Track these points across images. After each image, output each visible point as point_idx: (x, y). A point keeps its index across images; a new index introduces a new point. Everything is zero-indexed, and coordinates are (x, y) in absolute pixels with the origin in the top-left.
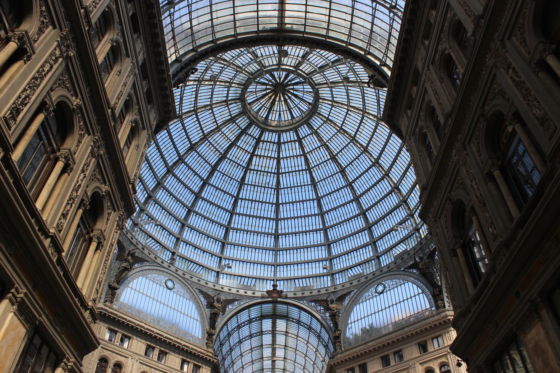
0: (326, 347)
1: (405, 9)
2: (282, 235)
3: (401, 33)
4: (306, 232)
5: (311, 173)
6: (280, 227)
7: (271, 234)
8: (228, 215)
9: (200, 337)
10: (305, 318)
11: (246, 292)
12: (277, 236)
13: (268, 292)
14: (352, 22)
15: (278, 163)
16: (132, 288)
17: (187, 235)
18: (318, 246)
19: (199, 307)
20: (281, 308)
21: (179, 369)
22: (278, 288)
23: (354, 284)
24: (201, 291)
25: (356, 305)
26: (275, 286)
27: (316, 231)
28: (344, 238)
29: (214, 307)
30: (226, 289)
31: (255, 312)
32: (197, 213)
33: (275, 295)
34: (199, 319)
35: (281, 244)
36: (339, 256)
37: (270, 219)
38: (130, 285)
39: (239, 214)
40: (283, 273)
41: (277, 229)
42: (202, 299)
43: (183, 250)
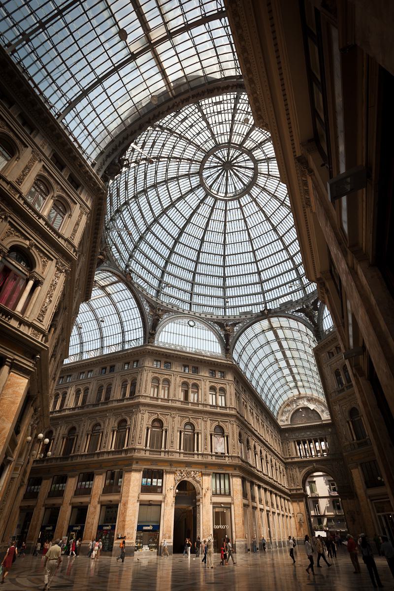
2: (262, 271)
4: (279, 264)
5: (270, 222)
7: (255, 273)
9: (220, 352)
10: (293, 324)
13: (261, 311)
15: (245, 221)
16: (165, 332)
17: (197, 289)
18: (289, 271)
20: (275, 322)
22: (268, 308)
27: (286, 261)
30: (232, 318)
31: (258, 327)
32: (200, 274)
34: (217, 341)
37: (251, 263)
38: (164, 330)
40: (269, 296)
41: (258, 269)
43: (196, 299)
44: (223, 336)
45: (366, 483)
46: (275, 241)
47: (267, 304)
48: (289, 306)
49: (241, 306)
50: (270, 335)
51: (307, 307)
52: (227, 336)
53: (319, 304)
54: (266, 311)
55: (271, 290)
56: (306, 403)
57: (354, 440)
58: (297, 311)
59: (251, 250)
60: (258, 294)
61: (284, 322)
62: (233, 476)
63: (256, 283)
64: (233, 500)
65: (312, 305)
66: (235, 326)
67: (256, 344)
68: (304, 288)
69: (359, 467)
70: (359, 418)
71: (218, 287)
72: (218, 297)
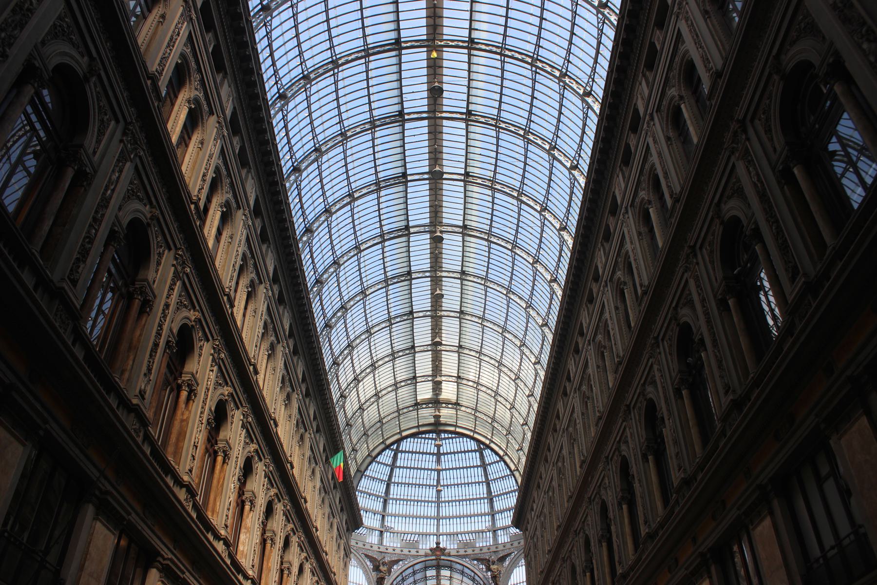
1: (621, 10)
3: (613, 52)
4: (468, 484)
6: (441, 478)
8: (388, 469)
13: (431, 550)
14: (542, 18)
18: (480, 499)
19: (365, 572)
22: (441, 546)
24: (366, 556)
26: (438, 543)
27: (479, 483)
28: (506, 493)
29: (381, 571)
33: (438, 553)
36: (502, 512)
39: (400, 467)
40: (446, 527)
42: (368, 563)
46: (472, 451)
59: (436, 452)
60: (431, 518)
68: (494, 531)
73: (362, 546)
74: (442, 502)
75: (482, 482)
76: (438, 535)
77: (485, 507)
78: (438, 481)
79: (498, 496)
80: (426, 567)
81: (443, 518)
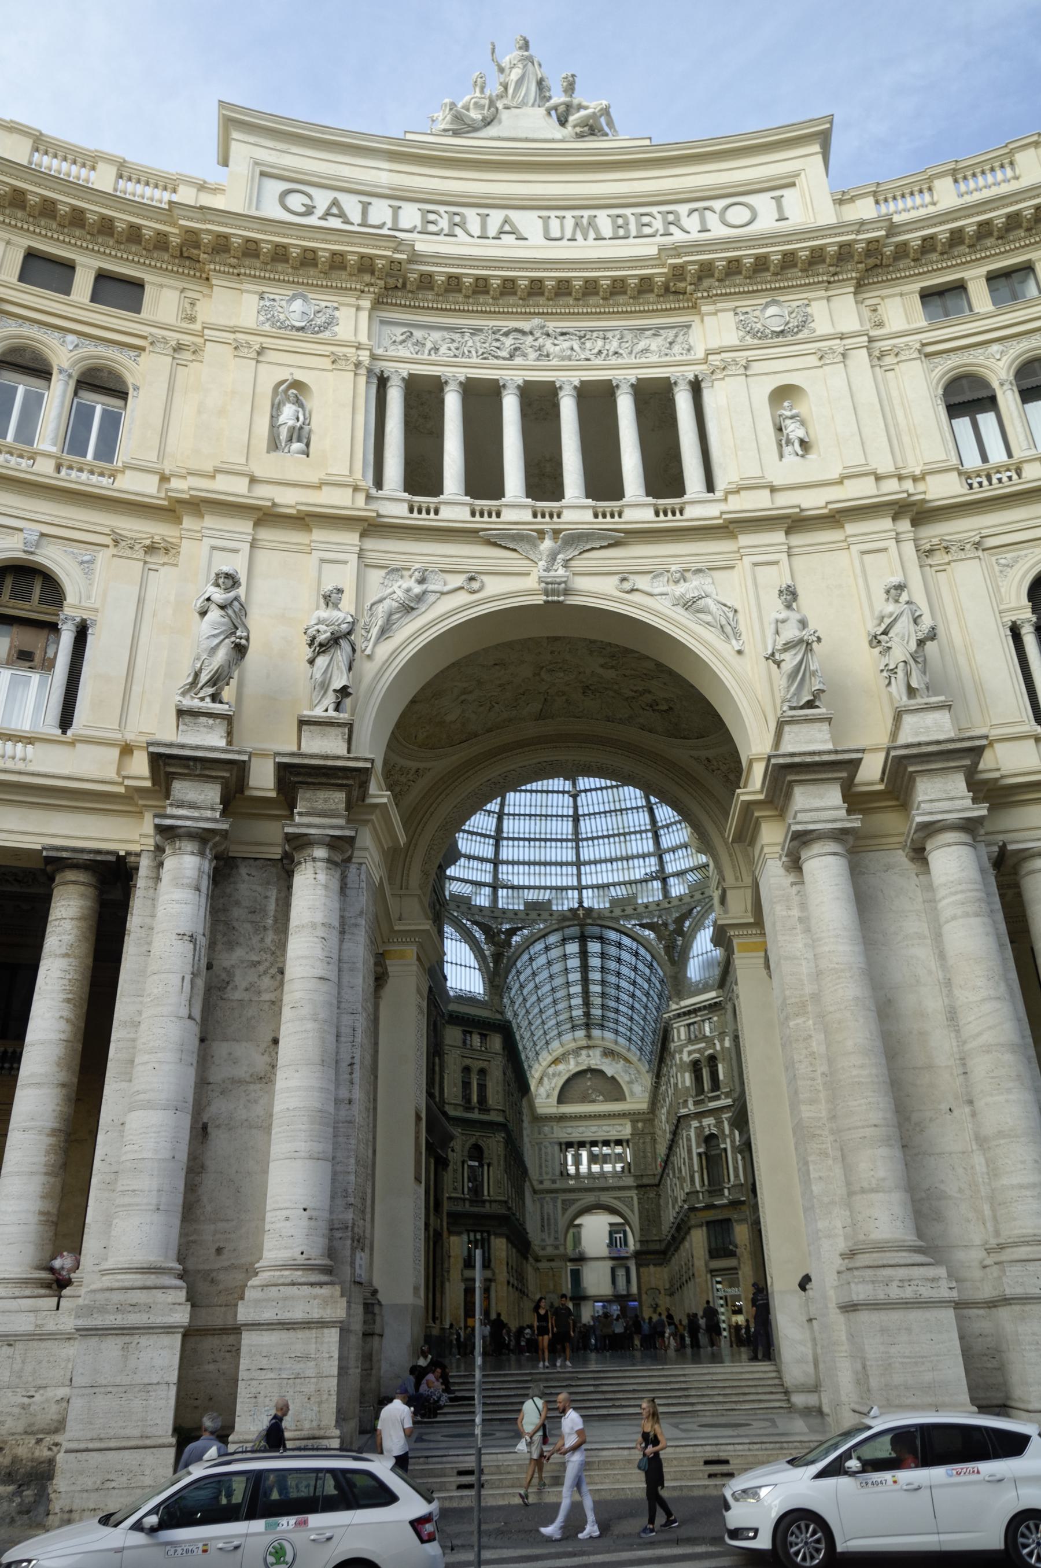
0: (662, 982)
2: (584, 815)
6: (579, 803)
9: (482, 992)
10: (626, 941)
11: (539, 915)
12: (576, 819)
13: (571, 910)
18: (641, 832)
21: (460, 1044)
22: (585, 905)
23: (696, 898)
25: (699, 930)
26: (581, 902)
34: (477, 966)
35: (583, 830)
36: (673, 850)
41: (576, 807)
44: (487, 953)
45: (710, 1252)
47: (584, 891)
48: (629, 910)
49: (529, 888)
50: (573, 948)
51: (665, 925)
52: (497, 957)
53: (687, 924)
54: (581, 912)
55: (595, 862)
56: (594, 1060)
57: (704, 1185)
58: (642, 926)
60: (567, 864)
61: (613, 935)
62: (497, 1235)
63: (567, 840)
64: (494, 1274)
65: (674, 922)
66: (515, 934)
67: (542, 960)
69: (704, 1228)
70: (718, 1152)
71: (485, 836)
72: (482, 860)
73: (466, 910)
74: (583, 840)
75: (642, 807)
76: (580, 888)
77: (649, 846)
78: (576, 807)
79: (668, 826)
80: (564, 940)
81: (585, 863)
